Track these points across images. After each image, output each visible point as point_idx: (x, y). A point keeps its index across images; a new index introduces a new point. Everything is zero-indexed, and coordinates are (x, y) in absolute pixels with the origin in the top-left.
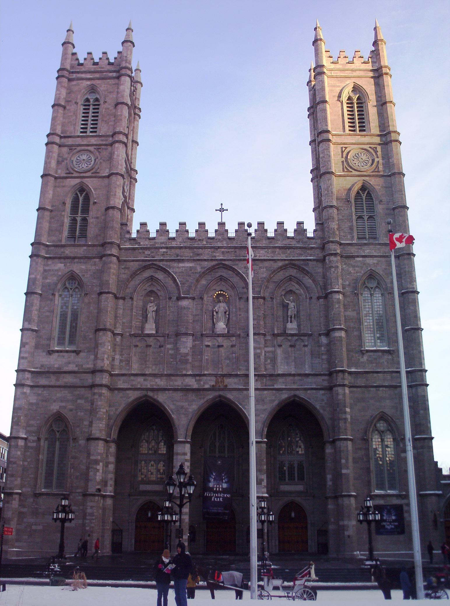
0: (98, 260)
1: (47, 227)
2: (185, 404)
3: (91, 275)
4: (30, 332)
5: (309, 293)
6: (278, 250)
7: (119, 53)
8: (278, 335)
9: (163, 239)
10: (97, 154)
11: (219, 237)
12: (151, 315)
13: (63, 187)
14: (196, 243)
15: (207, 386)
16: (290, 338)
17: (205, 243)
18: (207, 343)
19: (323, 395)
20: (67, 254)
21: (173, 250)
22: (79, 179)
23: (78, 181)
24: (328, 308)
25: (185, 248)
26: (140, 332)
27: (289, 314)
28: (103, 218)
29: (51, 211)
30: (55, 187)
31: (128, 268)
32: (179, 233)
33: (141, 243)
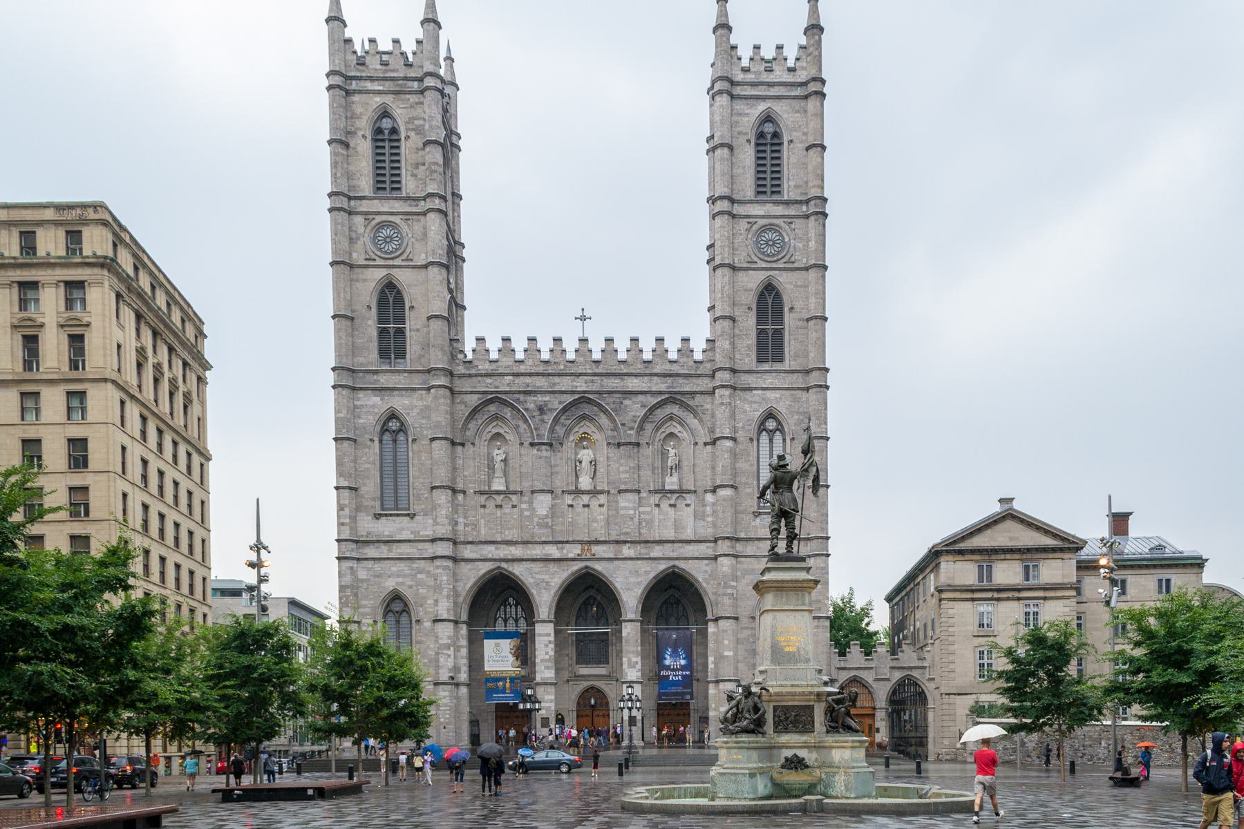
0: (424, 392)
1: (351, 343)
2: (546, 577)
3: (418, 413)
4: (347, 491)
5: (693, 436)
6: (656, 378)
7: (419, 42)
8: (656, 492)
9: (507, 361)
10: (406, 227)
11: (582, 359)
12: (499, 466)
13: (365, 280)
14: (550, 368)
15: (571, 556)
16: (669, 495)
17: (562, 367)
18: (570, 502)
19: (707, 565)
20: (383, 384)
21: (522, 378)
22: (385, 269)
23: (384, 272)
24: (714, 457)
25: (538, 374)
26: (487, 488)
27: (669, 464)
28: (425, 330)
29: (352, 319)
30: (351, 280)
31: (465, 403)
32: (529, 352)
33: (480, 367)
